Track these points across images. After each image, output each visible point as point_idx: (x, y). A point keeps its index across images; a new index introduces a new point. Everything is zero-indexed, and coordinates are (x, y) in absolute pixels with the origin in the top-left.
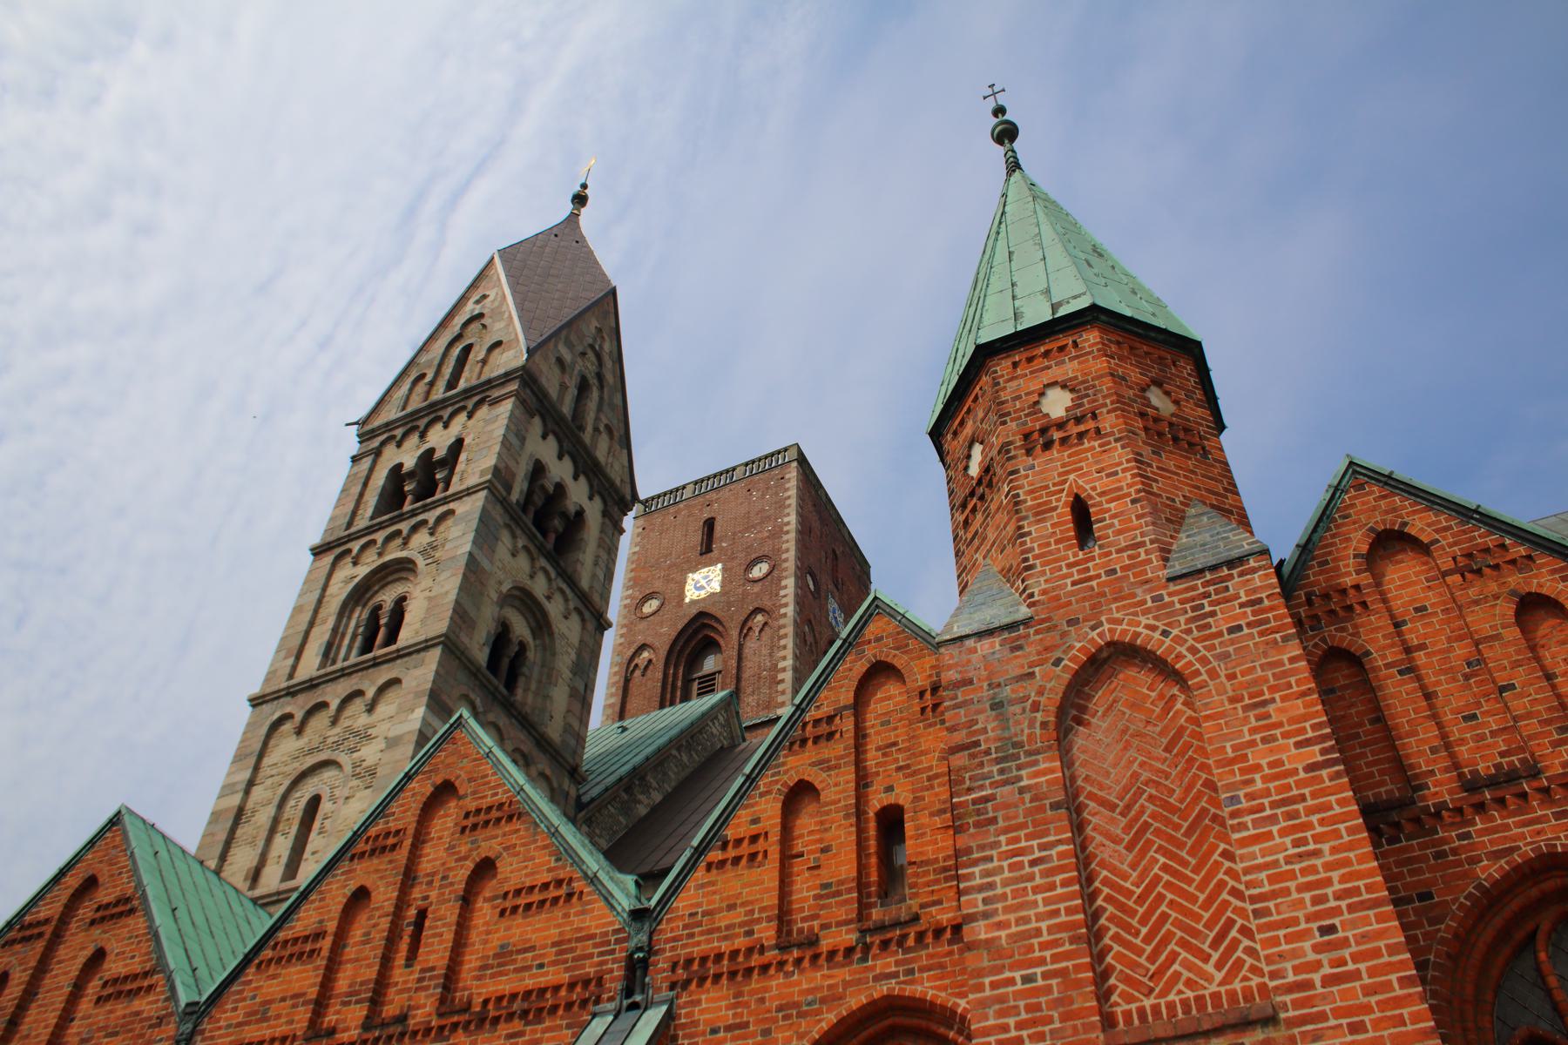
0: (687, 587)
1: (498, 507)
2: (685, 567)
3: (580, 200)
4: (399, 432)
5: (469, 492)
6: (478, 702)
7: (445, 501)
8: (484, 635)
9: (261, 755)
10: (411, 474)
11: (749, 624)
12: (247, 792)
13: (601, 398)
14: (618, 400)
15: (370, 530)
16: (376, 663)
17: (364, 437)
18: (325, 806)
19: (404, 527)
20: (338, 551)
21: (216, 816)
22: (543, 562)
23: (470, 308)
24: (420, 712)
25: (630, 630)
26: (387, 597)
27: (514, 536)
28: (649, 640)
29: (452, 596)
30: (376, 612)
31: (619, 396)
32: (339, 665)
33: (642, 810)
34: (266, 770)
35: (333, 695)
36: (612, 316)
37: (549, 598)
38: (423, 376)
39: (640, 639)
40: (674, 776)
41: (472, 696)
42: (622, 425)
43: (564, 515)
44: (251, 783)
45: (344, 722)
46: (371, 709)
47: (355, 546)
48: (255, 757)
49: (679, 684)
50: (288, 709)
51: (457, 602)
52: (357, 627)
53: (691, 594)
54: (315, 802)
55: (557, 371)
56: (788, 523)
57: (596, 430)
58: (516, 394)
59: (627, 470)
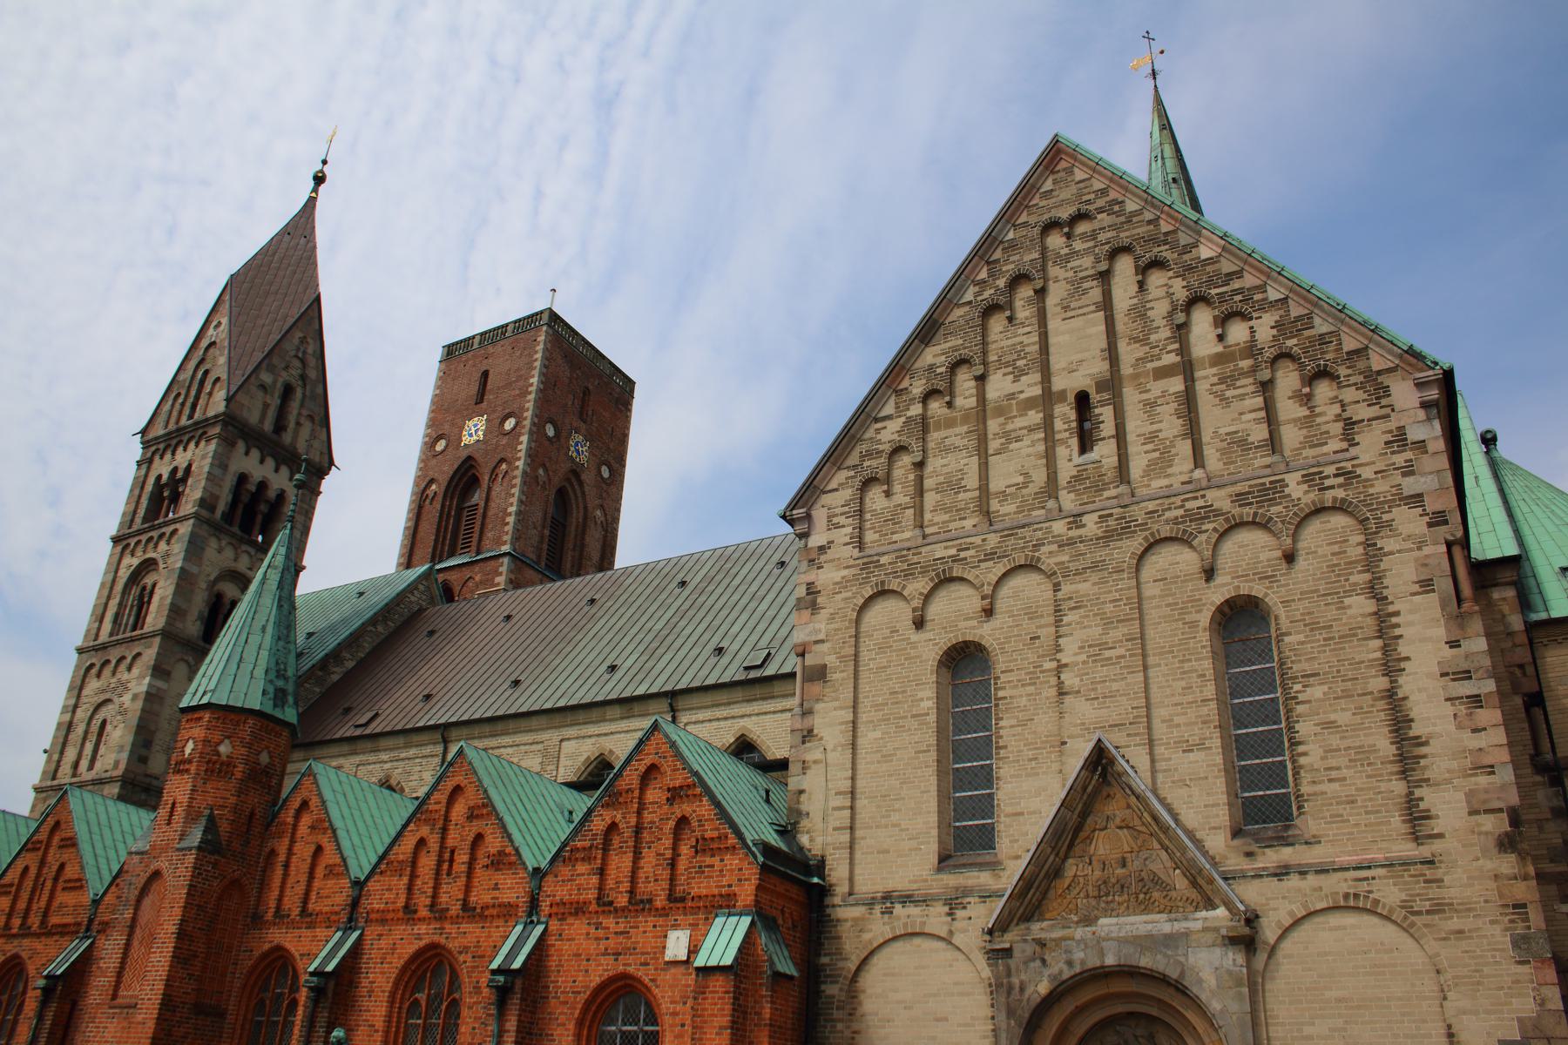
0: (464, 433)
1: (205, 527)
2: (465, 413)
3: (319, 179)
4: (162, 446)
5: (185, 518)
6: (190, 659)
7: (174, 521)
8: (196, 613)
9: (81, 689)
10: (166, 485)
11: (497, 470)
12: (74, 712)
13: (304, 395)
14: (320, 390)
15: (140, 532)
16: (132, 640)
17: (146, 444)
18: (109, 727)
19: (155, 534)
20: (125, 543)
21: (59, 725)
22: (244, 547)
23: (204, 343)
24: (148, 679)
25: (426, 466)
26: (148, 580)
27: (219, 540)
28: (436, 476)
29: (169, 601)
30: (144, 588)
31: (321, 386)
32: (119, 637)
33: (335, 678)
34: (83, 699)
35: (114, 655)
36: (317, 321)
37: (250, 569)
38: (179, 395)
39: (431, 474)
40: (367, 645)
41: (186, 658)
42: (323, 410)
43: (267, 501)
44: (76, 706)
45: (118, 675)
46: (129, 669)
47: (133, 542)
48: (77, 688)
49: (453, 513)
50: (94, 661)
51: (172, 604)
52: (133, 601)
53: (466, 440)
54: (104, 723)
55: (260, 394)
56: (532, 385)
57: (298, 424)
58: (219, 436)
59: (326, 444)
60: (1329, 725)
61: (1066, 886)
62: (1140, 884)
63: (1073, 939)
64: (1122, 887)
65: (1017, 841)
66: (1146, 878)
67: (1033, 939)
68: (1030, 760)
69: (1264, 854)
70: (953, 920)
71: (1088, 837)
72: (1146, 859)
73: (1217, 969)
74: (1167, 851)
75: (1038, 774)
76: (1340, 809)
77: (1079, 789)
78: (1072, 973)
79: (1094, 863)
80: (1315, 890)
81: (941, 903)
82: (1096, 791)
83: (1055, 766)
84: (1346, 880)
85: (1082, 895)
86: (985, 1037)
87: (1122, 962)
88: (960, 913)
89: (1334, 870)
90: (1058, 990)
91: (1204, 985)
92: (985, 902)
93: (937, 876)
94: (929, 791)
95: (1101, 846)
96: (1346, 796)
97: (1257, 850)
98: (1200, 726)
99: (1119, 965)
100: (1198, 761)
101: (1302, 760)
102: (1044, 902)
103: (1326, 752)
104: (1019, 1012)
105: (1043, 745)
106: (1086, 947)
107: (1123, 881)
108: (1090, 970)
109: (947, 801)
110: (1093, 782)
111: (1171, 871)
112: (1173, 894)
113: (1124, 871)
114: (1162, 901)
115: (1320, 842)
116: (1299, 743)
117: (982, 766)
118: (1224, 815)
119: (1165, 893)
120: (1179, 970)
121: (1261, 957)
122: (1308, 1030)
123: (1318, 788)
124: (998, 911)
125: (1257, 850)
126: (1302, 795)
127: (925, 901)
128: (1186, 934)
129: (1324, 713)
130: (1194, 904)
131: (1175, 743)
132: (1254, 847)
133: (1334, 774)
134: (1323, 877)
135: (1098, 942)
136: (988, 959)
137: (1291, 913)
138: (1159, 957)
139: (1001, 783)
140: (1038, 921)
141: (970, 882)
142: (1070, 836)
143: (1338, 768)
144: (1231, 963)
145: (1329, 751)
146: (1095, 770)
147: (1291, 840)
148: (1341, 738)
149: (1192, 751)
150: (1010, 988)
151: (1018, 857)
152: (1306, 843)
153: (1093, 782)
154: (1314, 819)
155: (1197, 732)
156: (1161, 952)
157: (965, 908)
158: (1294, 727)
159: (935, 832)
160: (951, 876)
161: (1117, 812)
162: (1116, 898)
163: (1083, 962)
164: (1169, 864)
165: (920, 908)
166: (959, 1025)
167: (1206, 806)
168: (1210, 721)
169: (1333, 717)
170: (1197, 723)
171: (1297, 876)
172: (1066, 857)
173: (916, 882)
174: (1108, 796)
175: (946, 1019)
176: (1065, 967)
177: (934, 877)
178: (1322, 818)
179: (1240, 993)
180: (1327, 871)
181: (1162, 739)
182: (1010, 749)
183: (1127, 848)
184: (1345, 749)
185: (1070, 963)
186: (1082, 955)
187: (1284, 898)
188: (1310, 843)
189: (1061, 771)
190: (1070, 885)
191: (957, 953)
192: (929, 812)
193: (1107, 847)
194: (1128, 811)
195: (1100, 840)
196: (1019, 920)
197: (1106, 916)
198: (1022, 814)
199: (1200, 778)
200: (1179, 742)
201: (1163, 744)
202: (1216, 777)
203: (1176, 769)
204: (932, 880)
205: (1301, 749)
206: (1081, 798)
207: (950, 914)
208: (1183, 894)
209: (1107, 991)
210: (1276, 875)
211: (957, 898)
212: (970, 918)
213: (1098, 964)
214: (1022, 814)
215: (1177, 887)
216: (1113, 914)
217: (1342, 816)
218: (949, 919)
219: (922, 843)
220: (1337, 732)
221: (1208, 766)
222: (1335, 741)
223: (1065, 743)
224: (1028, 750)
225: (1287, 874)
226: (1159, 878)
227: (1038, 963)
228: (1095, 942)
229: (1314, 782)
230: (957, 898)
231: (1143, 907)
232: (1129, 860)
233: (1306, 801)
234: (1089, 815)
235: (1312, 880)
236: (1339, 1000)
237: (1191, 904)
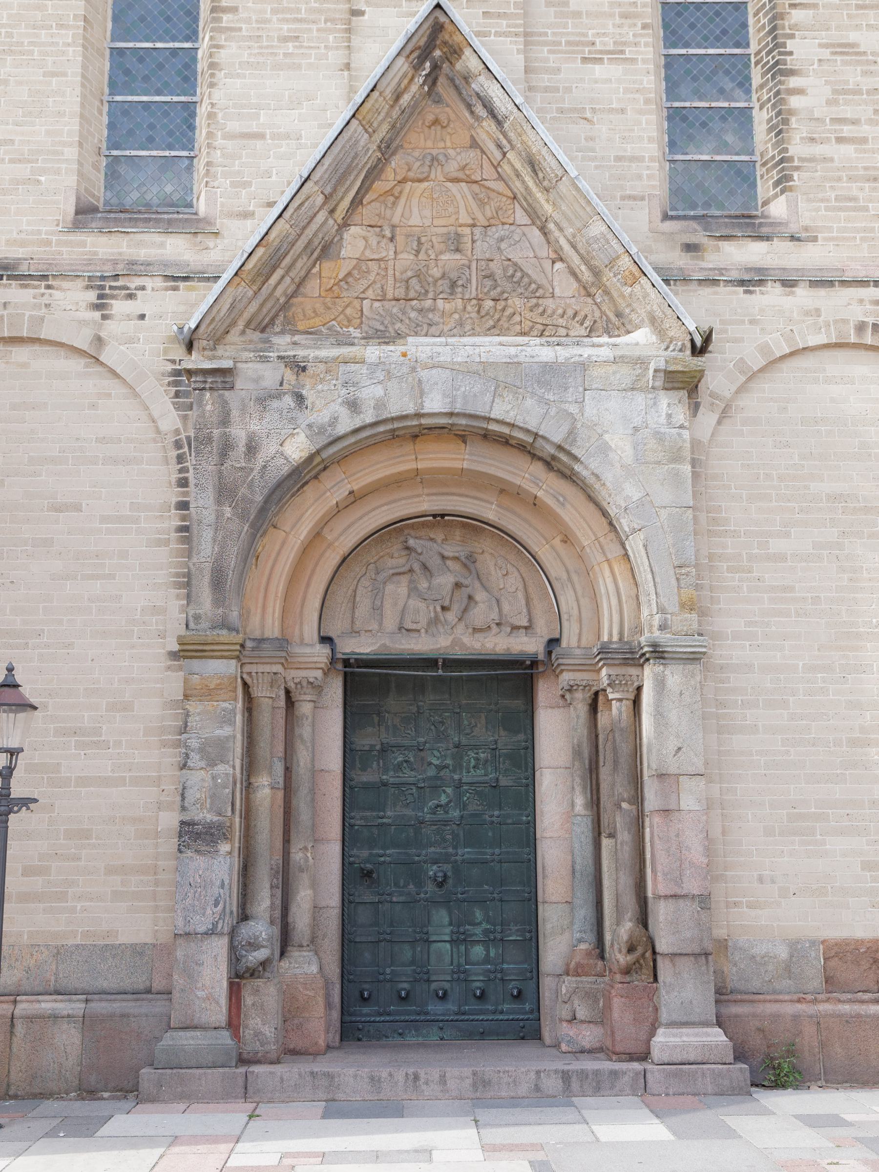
60: (846, 49)
61: (341, 276)
62: (488, 283)
63: (363, 362)
64: (453, 285)
65: (246, 184)
66: (499, 273)
67: (280, 357)
68: (285, 39)
69: (718, 249)
70: (105, 317)
71: (389, 192)
72: (502, 240)
73: (636, 429)
74: (544, 230)
75: (299, 67)
76: (854, 189)
77: (388, 93)
78: (358, 423)
79: (400, 239)
80: (807, 313)
81: (80, 283)
82: (414, 108)
83: (336, 57)
84: (861, 301)
85: (370, 293)
86: (160, 543)
87: (458, 408)
88: (119, 306)
89: (844, 283)
90: (325, 455)
91: (611, 455)
92: (175, 289)
93: (72, 237)
94: (64, 74)
95: (415, 210)
96: (866, 168)
97: (705, 241)
98: (618, 20)
99: (451, 414)
100: (609, 81)
101: (794, 102)
102: (294, 300)
103: (835, 92)
104: (243, 491)
105: (312, 17)
106: (389, 375)
107: (454, 275)
108: (393, 419)
109: (97, 103)
110: (414, 88)
111: (547, 264)
112: (549, 303)
113: (458, 256)
114: (528, 315)
115: (815, 239)
116: (792, 73)
117: (174, 52)
118: (649, 177)
119: (534, 301)
120: (565, 428)
121: (707, 419)
122: (777, 545)
123: (818, 150)
124: (204, 308)
125: (705, 241)
126: (790, 159)
127: (45, 277)
128: (583, 366)
129: (838, 28)
130: (587, 323)
131: (568, 43)
132: (700, 237)
133: (847, 130)
134: (822, 292)
135: (413, 369)
136: (177, 395)
137: (764, 349)
138: (529, 402)
139: (220, 75)
140: (282, 332)
141: (143, 254)
142: (358, 183)
143: (855, 122)
144: (663, 420)
145: (841, 92)
146: (422, 60)
147: (765, 230)
148: (865, 73)
149: (601, 60)
150: (226, 448)
151: (246, 215)
152: (793, 238)
153: (414, 88)
154: (809, 200)
155: (611, 29)
156: (533, 394)
157: (131, 296)
158: (784, 45)
159: (71, 153)
160: (103, 239)
161: (451, 152)
162: (440, 303)
163: (380, 405)
164: (544, 251)
165: (32, 291)
166: (104, 519)
167: (618, 159)
168: (636, 16)
169: (853, 36)
170: (612, 15)
171: (778, 289)
172: (345, 224)
173: (23, 244)
174: (436, 122)
175: (78, 508)
176: (344, 412)
177: (64, 238)
178: (822, 201)
179: (677, 474)
180: (831, 283)
181: (546, 34)
182: (243, 14)
183: (464, 218)
184: (869, 92)
185: (353, 405)
186: (379, 391)
187: (752, 322)
188: (799, 240)
189: (348, 66)
190: (349, 274)
191: (110, 384)
192: (61, 114)
193: (427, 213)
194: (473, 154)
195: (415, 201)
196: (248, 325)
197: (416, 334)
198: (261, 136)
199: (611, 111)
200: (577, 44)
201: (546, 44)
202: (640, 112)
203: (568, 90)
204: (59, 243)
205: (793, 82)
206: (387, 113)
207: (97, 307)
208: (569, 306)
209: (412, 466)
210: (742, 283)
211: (116, 277)
212: (142, 317)
213: (411, 409)
214: (261, 136)
215: (557, 292)
216: (433, 330)
217: (855, 199)
218: (97, 315)
219: (43, 171)
220: (858, 62)
221: (627, 91)
222: (853, 76)
223: (361, 13)
224: (280, 20)
225: (761, 282)
226: (525, 274)
227: (288, 400)
228: (405, 370)
229: (812, 140)
230: (116, 277)
231: (491, 323)
232: (468, 240)
233: (797, 168)
234: (394, 153)
235: (803, 295)
236: (834, 498)
237: (582, 324)
